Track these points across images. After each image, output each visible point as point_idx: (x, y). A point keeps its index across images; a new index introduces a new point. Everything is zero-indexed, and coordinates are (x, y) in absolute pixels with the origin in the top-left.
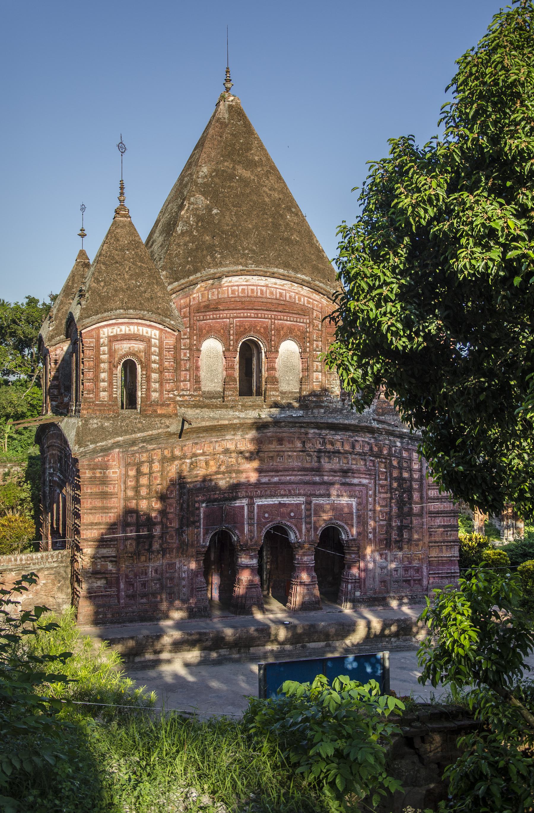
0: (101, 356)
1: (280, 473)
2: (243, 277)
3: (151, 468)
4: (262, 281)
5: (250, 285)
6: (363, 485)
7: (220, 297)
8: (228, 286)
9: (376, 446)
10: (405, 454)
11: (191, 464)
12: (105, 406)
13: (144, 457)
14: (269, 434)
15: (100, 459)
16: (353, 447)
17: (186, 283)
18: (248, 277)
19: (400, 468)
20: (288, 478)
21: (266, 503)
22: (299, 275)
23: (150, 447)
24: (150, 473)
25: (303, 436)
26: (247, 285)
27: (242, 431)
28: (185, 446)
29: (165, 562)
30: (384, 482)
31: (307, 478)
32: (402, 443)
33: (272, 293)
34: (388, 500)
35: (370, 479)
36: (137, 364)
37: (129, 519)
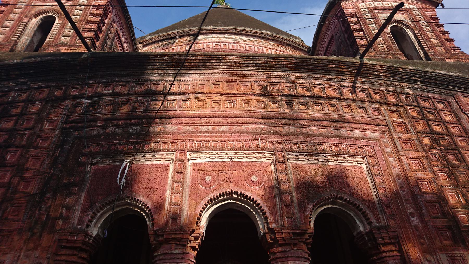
1: (230, 120)
2: (216, 36)
4: (234, 38)
5: (222, 42)
6: (373, 139)
7: (196, 49)
8: (202, 43)
9: (375, 93)
10: (423, 103)
14: (214, 77)
16: (341, 93)
17: (165, 36)
18: (220, 36)
19: (424, 118)
20: (244, 127)
21: (207, 160)
22: (263, 31)
23: (35, 85)
25: (263, 79)
26: (219, 42)
30: (407, 136)
31: (275, 129)
32: (412, 88)
33: (242, 47)
34: (425, 161)
35: (383, 132)
36: (57, 18)
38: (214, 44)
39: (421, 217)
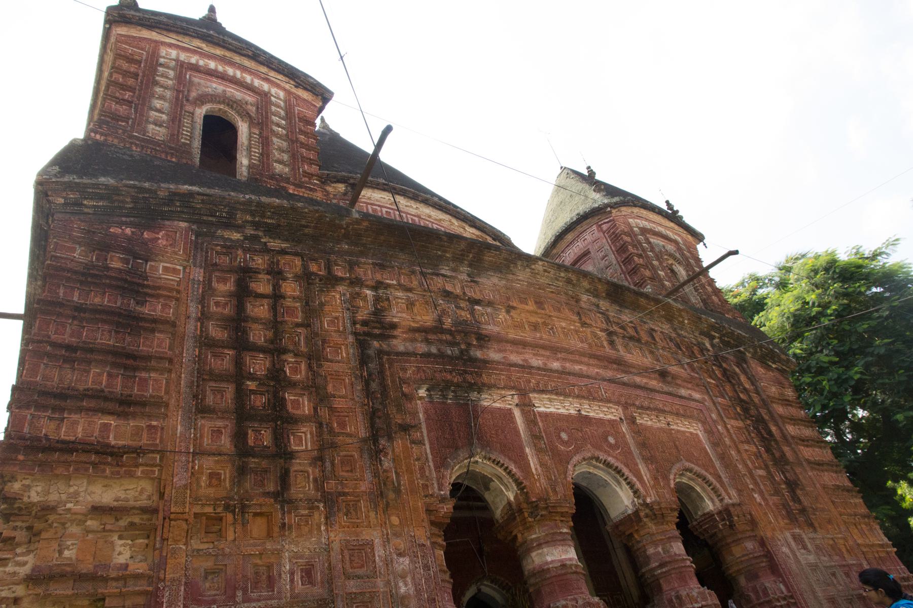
0: (157, 78)
3: (276, 287)
11: (377, 299)
12: (159, 146)
13: (260, 262)
15: (128, 231)
20: (577, 367)
21: (552, 410)
24: (277, 297)
27: (470, 266)
28: (358, 264)
29: (337, 537)
37: (210, 400)
38: (384, 210)
39: (761, 493)
